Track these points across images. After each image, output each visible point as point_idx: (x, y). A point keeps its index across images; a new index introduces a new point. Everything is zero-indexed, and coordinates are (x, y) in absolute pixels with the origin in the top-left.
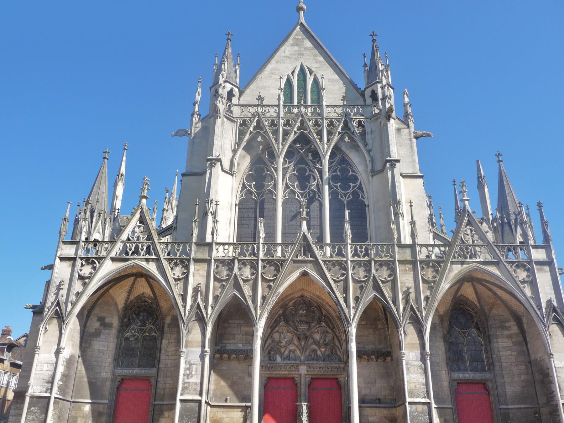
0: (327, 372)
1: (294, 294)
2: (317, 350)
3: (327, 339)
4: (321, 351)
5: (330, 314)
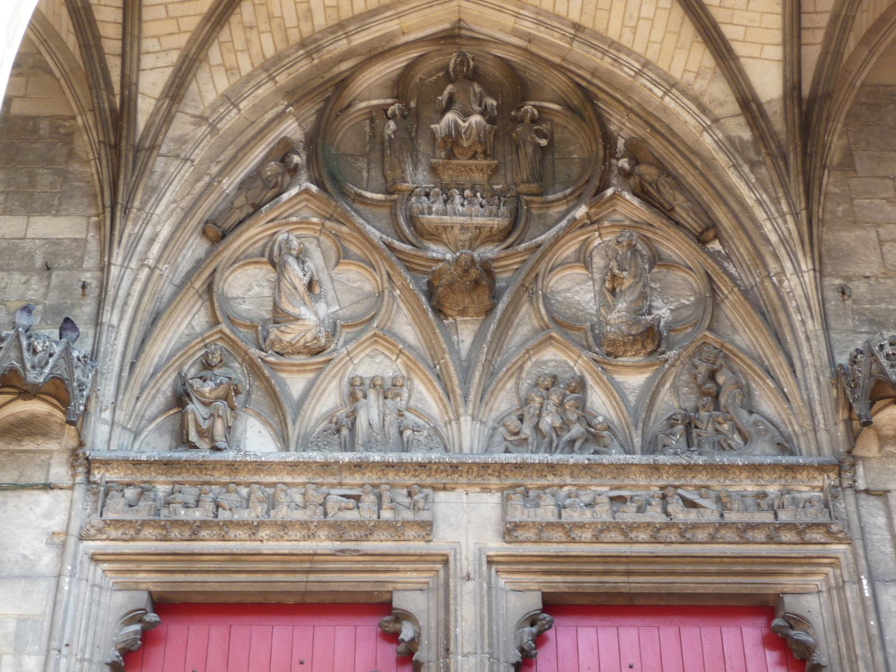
0: (686, 532)
1: (399, 15)
2: (581, 385)
3: (658, 303)
4: (616, 391)
5: (668, 135)
